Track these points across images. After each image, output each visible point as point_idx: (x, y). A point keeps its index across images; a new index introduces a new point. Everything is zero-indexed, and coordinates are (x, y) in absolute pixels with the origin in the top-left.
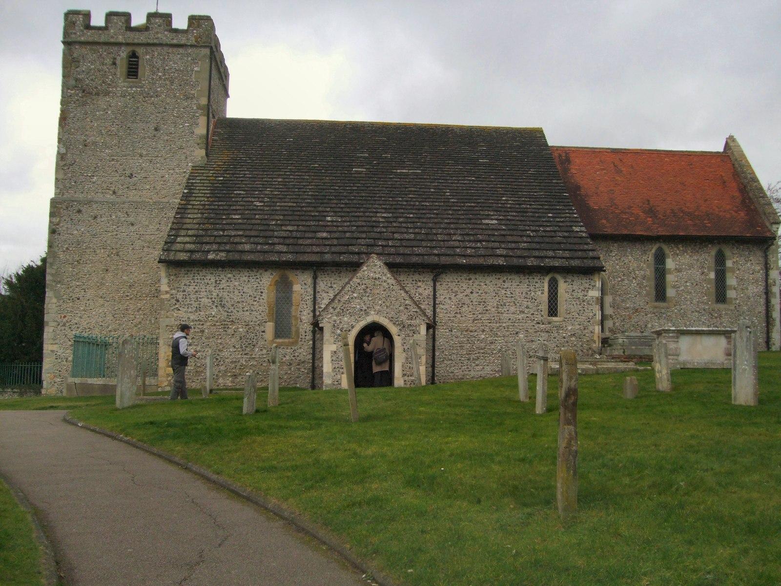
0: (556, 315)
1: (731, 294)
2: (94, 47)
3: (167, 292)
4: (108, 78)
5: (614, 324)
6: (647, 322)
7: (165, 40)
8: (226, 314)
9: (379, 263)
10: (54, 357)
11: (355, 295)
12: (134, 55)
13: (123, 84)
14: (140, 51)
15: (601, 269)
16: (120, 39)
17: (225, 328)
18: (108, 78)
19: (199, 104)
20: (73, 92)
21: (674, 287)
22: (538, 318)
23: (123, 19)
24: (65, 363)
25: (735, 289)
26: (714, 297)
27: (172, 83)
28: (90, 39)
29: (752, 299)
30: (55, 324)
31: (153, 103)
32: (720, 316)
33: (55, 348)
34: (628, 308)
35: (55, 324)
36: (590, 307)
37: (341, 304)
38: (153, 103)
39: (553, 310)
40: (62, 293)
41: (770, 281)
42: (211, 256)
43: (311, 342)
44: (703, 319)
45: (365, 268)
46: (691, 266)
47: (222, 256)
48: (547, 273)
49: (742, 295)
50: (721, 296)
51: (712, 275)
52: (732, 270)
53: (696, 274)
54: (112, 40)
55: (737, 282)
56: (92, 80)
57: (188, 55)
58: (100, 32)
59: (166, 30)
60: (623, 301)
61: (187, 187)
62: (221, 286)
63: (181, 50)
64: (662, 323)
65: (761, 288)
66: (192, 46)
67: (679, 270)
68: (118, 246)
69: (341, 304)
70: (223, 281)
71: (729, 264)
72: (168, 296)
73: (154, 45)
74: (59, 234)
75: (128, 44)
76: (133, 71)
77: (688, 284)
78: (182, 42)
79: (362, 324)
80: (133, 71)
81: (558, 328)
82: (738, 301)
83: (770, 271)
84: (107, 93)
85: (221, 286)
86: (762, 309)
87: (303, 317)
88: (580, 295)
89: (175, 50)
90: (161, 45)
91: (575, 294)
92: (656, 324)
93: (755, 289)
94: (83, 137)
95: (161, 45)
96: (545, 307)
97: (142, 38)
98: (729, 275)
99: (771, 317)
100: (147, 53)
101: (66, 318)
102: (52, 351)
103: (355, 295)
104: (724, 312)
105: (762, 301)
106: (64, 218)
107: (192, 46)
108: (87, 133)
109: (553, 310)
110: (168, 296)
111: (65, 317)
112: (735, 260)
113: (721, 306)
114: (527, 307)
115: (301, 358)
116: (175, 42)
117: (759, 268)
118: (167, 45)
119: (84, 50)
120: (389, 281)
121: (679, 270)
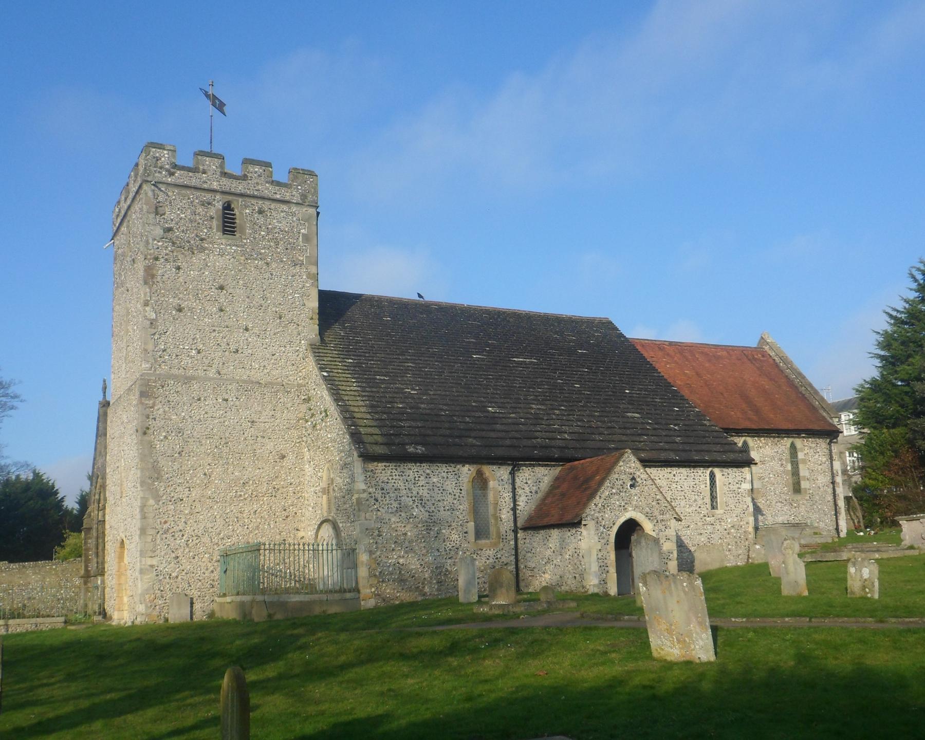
1: (804, 484)
2: (184, 191)
3: (364, 491)
4: (202, 231)
7: (266, 193)
8: (427, 514)
9: (633, 458)
10: (155, 574)
11: (614, 491)
12: (227, 207)
13: (220, 240)
15: (748, 463)
16: (215, 185)
17: (429, 529)
18: (202, 231)
19: (309, 273)
20: (160, 244)
22: (704, 512)
23: (217, 162)
24: (167, 580)
26: (792, 488)
27: (277, 244)
28: (180, 182)
30: (153, 532)
31: (256, 267)
33: (154, 562)
35: (153, 532)
36: (744, 499)
37: (602, 500)
38: (256, 267)
40: (161, 493)
42: (411, 449)
43: (512, 543)
45: (621, 463)
46: (773, 458)
47: (420, 449)
48: (709, 467)
50: (797, 489)
51: (789, 467)
52: (804, 461)
53: (776, 465)
54: (205, 186)
56: (183, 231)
57: (293, 214)
58: (191, 174)
59: (267, 182)
61: (321, 369)
62: (421, 483)
63: (285, 207)
65: (829, 478)
66: (297, 204)
68: (227, 435)
69: (602, 500)
70: (422, 478)
71: (801, 455)
72: (365, 495)
73: (254, 197)
74: (155, 419)
75: (223, 193)
76: (228, 224)
78: (287, 198)
79: (622, 520)
80: (228, 224)
81: (720, 520)
84: (203, 249)
85: (421, 483)
86: (830, 498)
87: (503, 516)
88: (735, 487)
89: (278, 205)
90: (263, 198)
91: (731, 486)
93: (823, 480)
94: (177, 301)
95: (263, 198)
97: (240, 187)
98: (801, 466)
100: (246, 207)
101: (167, 525)
102: (152, 566)
103: (614, 491)
105: (830, 490)
106: (160, 399)
107: (297, 204)
108: (181, 296)
110: (365, 495)
111: (166, 522)
114: (695, 500)
115: (504, 559)
116: (278, 196)
118: (269, 199)
119: (173, 193)
120: (642, 476)
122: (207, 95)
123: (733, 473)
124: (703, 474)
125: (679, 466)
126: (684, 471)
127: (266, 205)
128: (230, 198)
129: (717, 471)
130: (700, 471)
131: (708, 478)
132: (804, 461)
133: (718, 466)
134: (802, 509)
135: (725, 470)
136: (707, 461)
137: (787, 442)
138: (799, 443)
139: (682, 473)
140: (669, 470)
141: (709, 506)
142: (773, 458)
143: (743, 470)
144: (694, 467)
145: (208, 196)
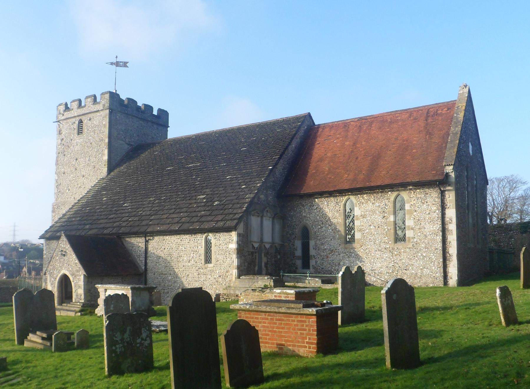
0: (211, 263)
5: (316, 262)
7: (93, 110)
12: (81, 122)
14: (83, 118)
21: (360, 230)
25: (412, 229)
29: (429, 237)
32: (399, 254)
34: (325, 249)
39: (208, 259)
41: (447, 219)
44: (385, 256)
46: (374, 212)
48: (205, 233)
49: (419, 234)
52: (410, 212)
53: (378, 218)
55: (415, 222)
60: (322, 244)
63: (98, 114)
64: (352, 261)
65: (438, 226)
67: (363, 216)
77: (372, 227)
82: (415, 240)
83: (446, 210)
92: (347, 262)
96: (203, 257)
99: (448, 253)
104: (403, 250)
105: (439, 238)
109: (208, 259)
112: (412, 203)
113: (400, 245)
117: (435, 208)
121: (363, 216)
122: (112, 64)
123: (223, 236)
124: (200, 239)
125: (184, 234)
126: (187, 236)
127: (90, 116)
128: (80, 118)
129: (211, 236)
130: (199, 236)
131: (203, 241)
132: (410, 212)
134: (404, 256)
135: (217, 234)
137: (392, 195)
138: (405, 195)
139: (186, 238)
140: (178, 236)
141: (203, 261)
142: (374, 212)
143: (231, 234)
144: (195, 234)
145: (74, 120)
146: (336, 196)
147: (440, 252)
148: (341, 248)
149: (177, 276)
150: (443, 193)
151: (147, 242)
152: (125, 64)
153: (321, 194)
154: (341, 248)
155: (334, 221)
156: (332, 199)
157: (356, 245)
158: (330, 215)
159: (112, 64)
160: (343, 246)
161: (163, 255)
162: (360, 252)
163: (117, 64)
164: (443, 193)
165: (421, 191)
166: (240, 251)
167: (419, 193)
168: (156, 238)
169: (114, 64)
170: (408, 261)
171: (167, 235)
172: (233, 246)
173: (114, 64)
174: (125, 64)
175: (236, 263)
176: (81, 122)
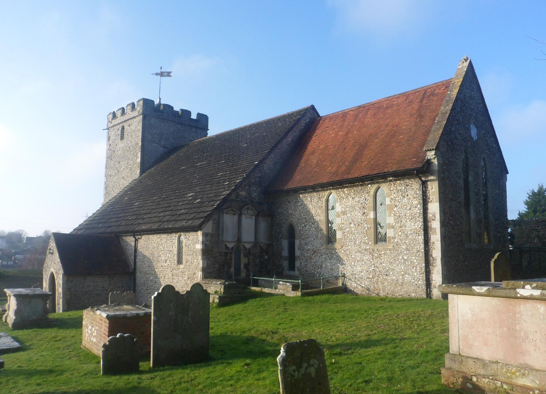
5: (301, 263)
6: (322, 262)
12: (123, 128)
25: (393, 227)
29: (410, 237)
34: (309, 250)
41: (430, 215)
48: (178, 232)
49: (400, 233)
53: (358, 215)
55: (395, 219)
60: (306, 244)
63: (135, 120)
64: (333, 264)
65: (420, 224)
77: (352, 225)
82: (396, 240)
83: (429, 204)
92: (329, 264)
99: (432, 255)
104: (383, 252)
105: (421, 238)
112: (392, 197)
113: (380, 245)
117: (416, 202)
122: (157, 74)
124: (174, 237)
126: (164, 236)
127: (129, 122)
133: (183, 231)
134: (384, 258)
136: (176, 228)
138: (385, 188)
142: (353, 207)
144: (171, 233)
145: (118, 127)
146: (319, 191)
147: (422, 254)
148: (323, 249)
149: (156, 277)
150: (424, 184)
151: (136, 240)
152: (169, 74)
153: (306, 189)
154: (323, 249)
155: (317, 218)
156: (315, 194)
157: (337, 245)
158: (313, 212)
159: (157, 74)
160: (324, 246)
161: (147, 255)
162: (341, 253)
163: (162, 74)
164: (424, 184)
165: (402, 182)
166: (206, 252)
167: (400, 185)
168: (143, 237)
169: (159, 74)
170: (388, 265)
171: (150, 234)
172: (199, 246)
173: (159, 74)
174: (169, 74)
175: (201, 265)
176: (123, 128)
